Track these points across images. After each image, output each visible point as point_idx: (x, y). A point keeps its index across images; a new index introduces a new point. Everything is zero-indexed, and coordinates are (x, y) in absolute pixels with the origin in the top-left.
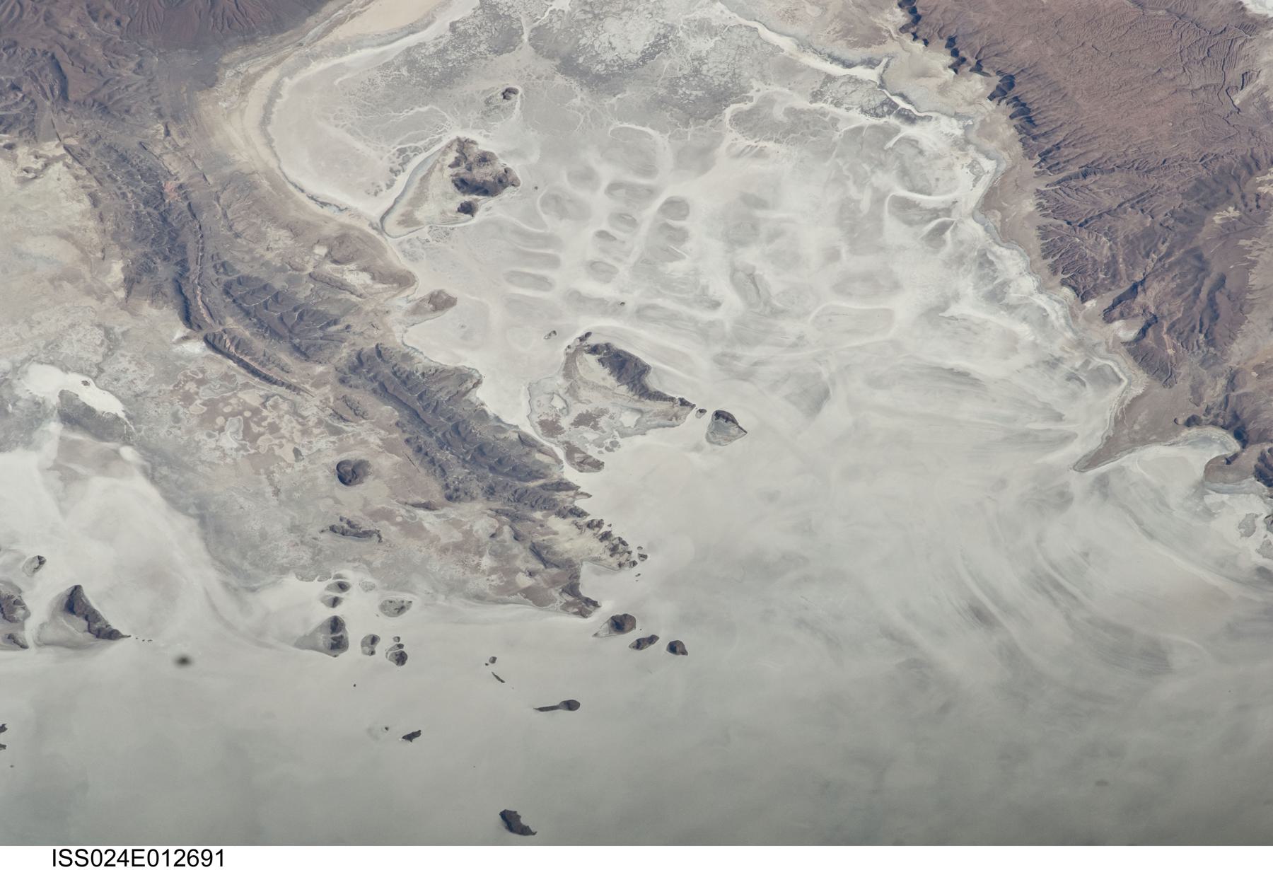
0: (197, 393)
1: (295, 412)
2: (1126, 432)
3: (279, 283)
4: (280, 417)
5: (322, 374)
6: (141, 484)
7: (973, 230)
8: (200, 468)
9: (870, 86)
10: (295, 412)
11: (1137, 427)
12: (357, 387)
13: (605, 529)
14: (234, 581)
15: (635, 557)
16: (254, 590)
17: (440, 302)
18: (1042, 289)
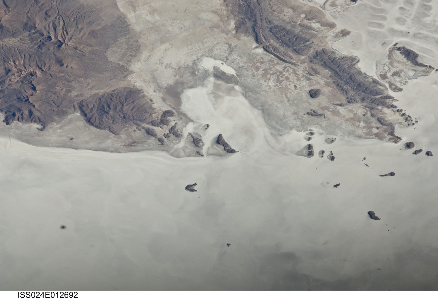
0: (261, 67)
1: (295, 72)
3: (288, 28)
4: (289, 74)
5: (304, 59)
6: (242, 99)
8: (262, 93)
10: (295, 72)
12: (316, 63)
13: (403, 112)
14: (274, 132)
16: (281, 135)
17: (345, 33)
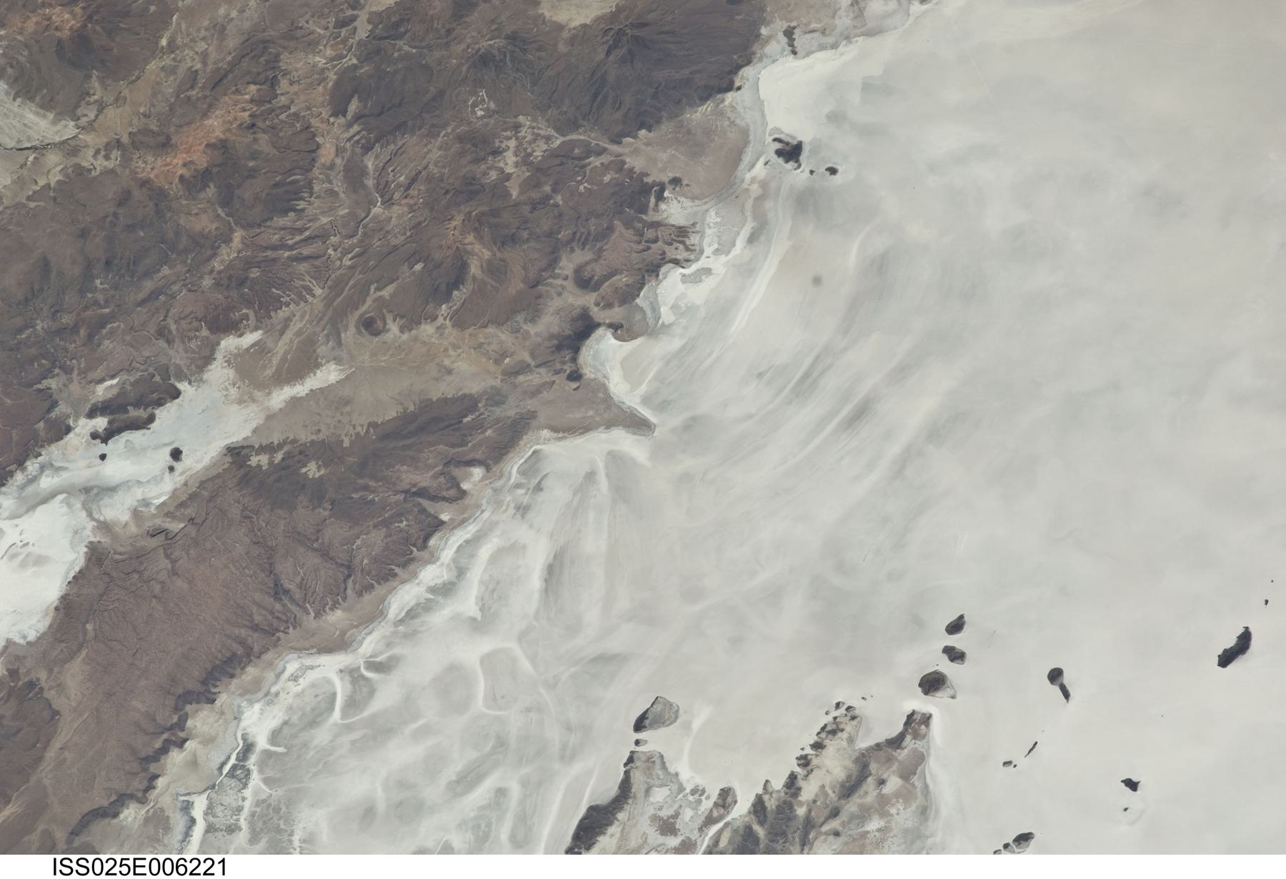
2: (597, 419)
7: (370, 644)
9: (213, 795)
11: (591, 413)
13: (809, 751)
15: (842, 710)
18: (433, 559)
